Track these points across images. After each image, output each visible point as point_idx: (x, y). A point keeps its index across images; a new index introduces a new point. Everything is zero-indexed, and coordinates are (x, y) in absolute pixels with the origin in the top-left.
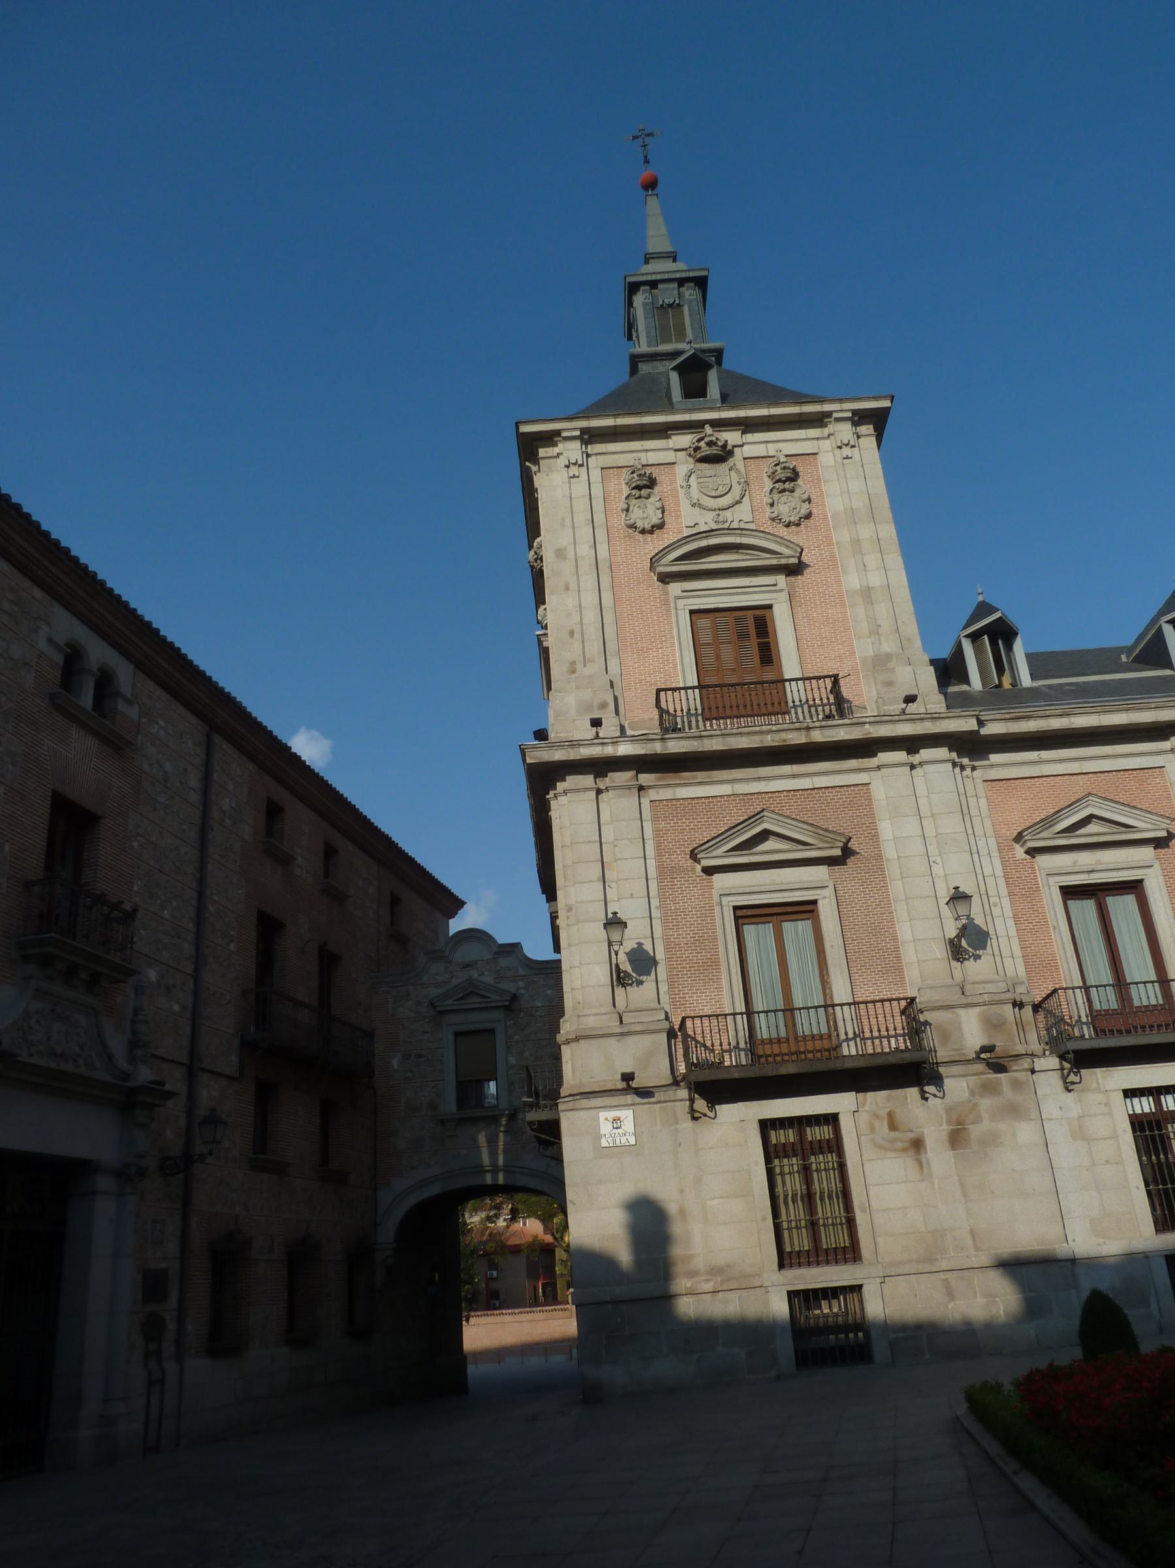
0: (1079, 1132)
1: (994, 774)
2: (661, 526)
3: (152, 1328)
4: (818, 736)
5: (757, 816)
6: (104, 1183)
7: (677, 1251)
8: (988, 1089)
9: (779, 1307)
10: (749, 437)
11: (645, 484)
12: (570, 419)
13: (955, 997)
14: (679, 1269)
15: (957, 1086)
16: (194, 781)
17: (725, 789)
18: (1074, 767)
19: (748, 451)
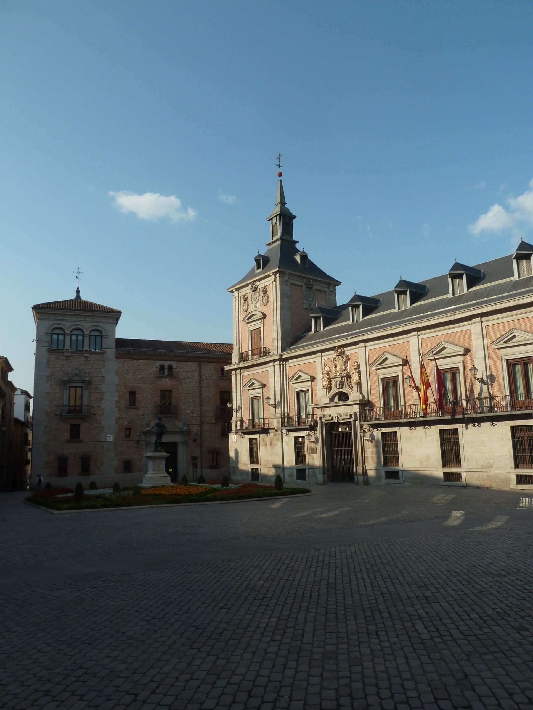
0: (287, 445)
1: (290, 365)
2: (248, 309)
3: (195, 465)
4: (259, 362)
5: (250, 380)
6: (179, 445)
7: (239, 460)
8: (276, 435)
9: (250, 470)
10: (261, 282)
11: (246, 299)
12: (233, 287)
13: (273, 416)
14: (239, 463)
15: (272, 433)
16: (197, 374)
17: (250, 373)
18: (301, 363)
19: (261, 286)
